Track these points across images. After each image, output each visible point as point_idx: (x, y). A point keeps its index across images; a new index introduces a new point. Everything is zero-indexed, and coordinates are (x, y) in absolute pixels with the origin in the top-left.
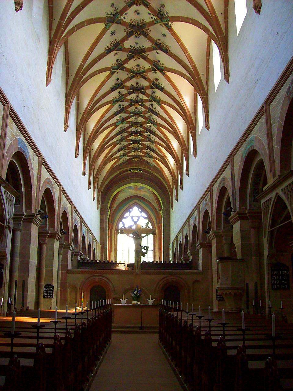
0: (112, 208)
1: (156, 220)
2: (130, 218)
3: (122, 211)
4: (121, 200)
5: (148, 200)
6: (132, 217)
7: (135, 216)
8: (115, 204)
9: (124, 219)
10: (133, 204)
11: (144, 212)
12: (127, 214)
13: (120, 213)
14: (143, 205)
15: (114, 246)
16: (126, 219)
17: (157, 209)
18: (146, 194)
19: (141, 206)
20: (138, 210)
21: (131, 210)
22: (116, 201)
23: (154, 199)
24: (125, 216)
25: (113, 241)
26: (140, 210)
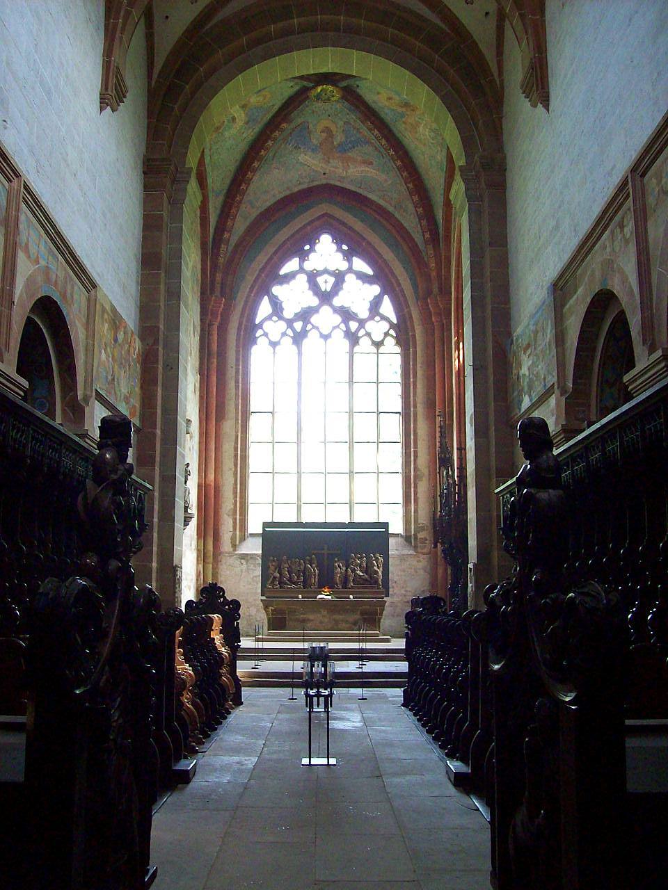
0: (226, 236)
1: (415, 286)
2: (302, 279)
3: (270, 250)
4: (268, 201)
5: (381, 202)
6: (312, 277)
7: (326, 271)
8: (238, 218)
9: (281, 283)
10: (317, 223)
11: (359, 258)
12: (292, 265)
13: (262, 258)
14: (358, 226)
15: (237, 395)
16: (285, 286)
17: (418, 238)
18: (370, 172)
19: (350, 228)
20: (334, 247)
21: (307, 247)
22: (243, 206)
23: (406, 193)
24: (283, 271)
25: (231, 373)
26: (345, 247)
